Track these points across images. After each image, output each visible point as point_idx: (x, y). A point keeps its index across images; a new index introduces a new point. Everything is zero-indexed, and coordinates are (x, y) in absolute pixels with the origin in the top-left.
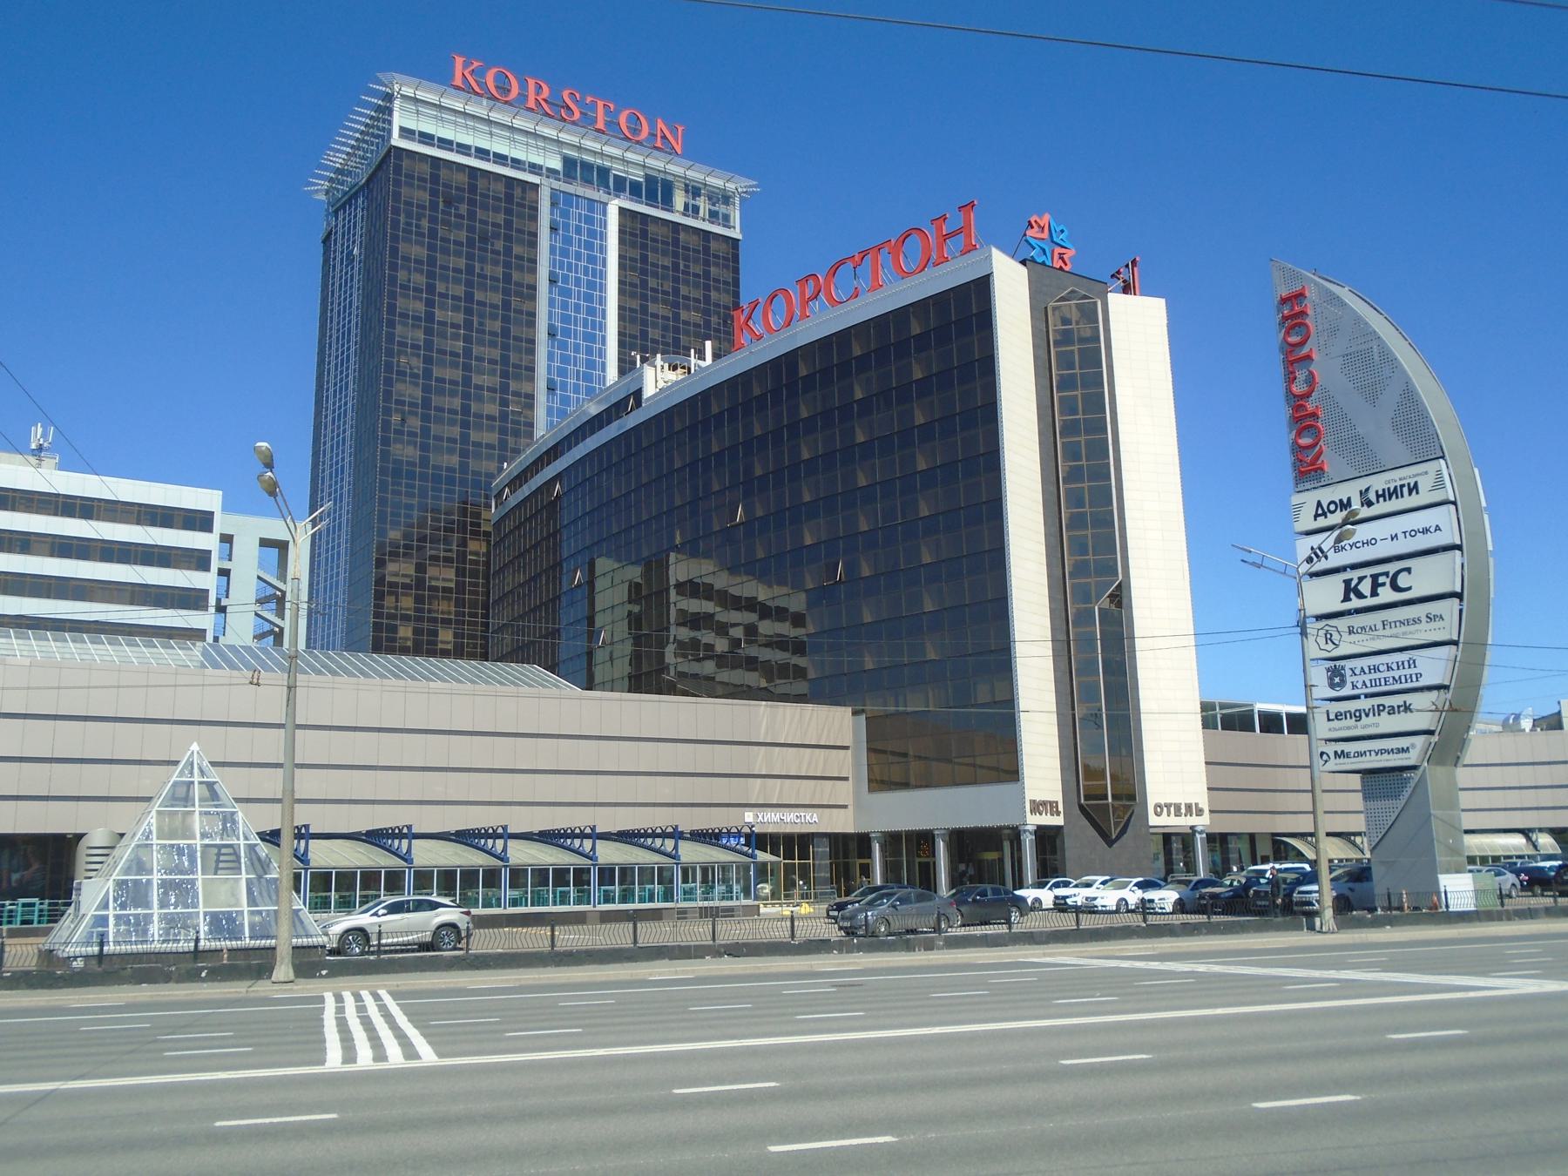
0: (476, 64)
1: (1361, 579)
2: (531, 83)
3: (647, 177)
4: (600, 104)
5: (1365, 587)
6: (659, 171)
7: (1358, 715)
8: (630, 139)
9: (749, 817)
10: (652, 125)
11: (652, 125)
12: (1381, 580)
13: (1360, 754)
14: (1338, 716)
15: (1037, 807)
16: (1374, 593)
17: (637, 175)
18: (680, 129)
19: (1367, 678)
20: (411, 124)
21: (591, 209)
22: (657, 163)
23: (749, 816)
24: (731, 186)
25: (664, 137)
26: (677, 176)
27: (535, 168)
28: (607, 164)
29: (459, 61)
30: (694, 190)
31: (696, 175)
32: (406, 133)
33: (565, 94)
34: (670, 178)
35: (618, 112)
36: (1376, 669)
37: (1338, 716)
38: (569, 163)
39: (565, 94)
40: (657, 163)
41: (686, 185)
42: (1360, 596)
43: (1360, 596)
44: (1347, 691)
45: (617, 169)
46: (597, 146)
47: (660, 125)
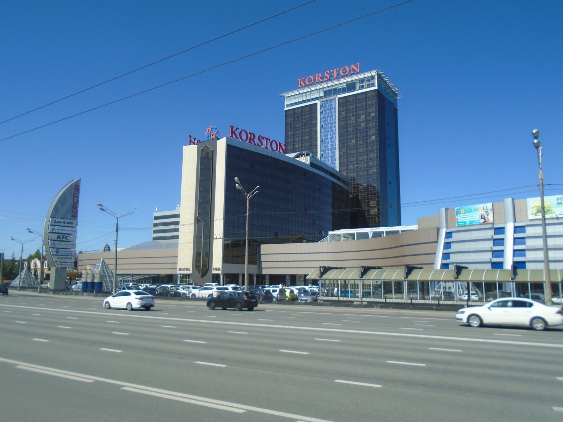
0: (303, 79)
1: (61, 236)
2: (317, 75)
3: (347, 85)
4: (335, 70)
5: (61, 237)
6: (351, 81)
8: (339, 77)
10: (350, 68)
11: (350, 68)
12: (64, 237)
13: (65, 265)
14: (59, 258)
15: (180, 269)
16: (63, 239)
17: (345, 86)
19: (63, 252)
20: (288, 103)
21: (331, 102)
22: (349, 79)
25: (354, 70)
27: (317, 99)
28: (336, 87)
29: (299, 80)
30: (362, 81)
31: (361, 76)
32: (287, 106)
33: (326, 74)
34: (354, 81)
35: (340, 70)
36: (65, 251)
37: (59, 258)
38: (325, 92)
39: (326, 74)
40: (349, 79)
41: (360, 81)
42: (60, 238)
43: (60, 238)
44: (59, 254)
45: (339, 87)
46: (332, 84)
47: (353, 66)
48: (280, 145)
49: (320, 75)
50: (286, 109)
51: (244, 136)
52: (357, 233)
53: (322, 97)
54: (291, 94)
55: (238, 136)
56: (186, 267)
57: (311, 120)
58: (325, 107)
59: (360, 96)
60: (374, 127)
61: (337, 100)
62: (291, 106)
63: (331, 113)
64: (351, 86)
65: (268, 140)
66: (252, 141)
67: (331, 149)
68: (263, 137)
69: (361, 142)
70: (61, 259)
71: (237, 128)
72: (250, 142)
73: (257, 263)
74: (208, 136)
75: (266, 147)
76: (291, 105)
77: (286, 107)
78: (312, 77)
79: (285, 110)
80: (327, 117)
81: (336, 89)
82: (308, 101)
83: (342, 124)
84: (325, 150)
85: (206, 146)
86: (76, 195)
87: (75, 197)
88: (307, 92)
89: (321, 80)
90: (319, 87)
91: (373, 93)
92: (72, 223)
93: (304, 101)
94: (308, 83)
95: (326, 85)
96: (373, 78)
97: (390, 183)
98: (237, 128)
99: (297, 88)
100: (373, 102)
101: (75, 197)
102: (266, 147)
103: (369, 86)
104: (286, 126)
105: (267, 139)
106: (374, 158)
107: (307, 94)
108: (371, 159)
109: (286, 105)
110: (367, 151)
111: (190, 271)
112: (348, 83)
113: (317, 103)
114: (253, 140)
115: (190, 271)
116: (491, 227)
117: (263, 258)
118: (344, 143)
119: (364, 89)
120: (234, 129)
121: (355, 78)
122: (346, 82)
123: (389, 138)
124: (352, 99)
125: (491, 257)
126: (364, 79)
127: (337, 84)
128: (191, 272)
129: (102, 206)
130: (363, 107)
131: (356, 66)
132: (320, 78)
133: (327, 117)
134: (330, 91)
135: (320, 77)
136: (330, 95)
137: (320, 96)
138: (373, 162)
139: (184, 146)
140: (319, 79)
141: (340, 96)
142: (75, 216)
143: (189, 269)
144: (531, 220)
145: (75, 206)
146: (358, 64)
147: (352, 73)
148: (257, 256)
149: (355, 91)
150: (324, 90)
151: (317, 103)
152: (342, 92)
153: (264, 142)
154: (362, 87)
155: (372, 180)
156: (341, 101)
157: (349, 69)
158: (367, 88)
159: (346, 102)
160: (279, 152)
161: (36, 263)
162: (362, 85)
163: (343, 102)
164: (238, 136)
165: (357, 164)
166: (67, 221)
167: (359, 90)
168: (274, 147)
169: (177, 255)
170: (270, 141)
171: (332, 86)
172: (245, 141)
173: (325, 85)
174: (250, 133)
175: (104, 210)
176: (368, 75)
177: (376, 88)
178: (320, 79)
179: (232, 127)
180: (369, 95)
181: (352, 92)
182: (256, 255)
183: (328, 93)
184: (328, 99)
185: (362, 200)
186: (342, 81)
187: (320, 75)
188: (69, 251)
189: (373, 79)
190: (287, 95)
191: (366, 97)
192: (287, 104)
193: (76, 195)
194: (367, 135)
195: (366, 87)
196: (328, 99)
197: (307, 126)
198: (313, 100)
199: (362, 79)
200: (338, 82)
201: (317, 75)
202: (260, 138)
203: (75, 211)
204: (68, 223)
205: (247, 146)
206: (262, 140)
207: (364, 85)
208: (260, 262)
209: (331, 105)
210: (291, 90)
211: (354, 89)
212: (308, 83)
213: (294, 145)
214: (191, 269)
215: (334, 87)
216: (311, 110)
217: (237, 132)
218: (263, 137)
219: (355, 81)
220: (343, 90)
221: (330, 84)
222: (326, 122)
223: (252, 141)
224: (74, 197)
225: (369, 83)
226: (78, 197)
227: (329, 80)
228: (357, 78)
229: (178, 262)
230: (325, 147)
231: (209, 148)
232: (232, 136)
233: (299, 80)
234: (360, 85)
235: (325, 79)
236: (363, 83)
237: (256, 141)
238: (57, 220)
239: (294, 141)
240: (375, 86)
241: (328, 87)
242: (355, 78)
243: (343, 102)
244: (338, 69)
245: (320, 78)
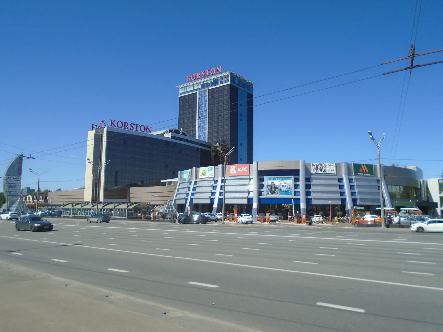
0: (190, 76)
3: (214, 81)
4: (207, 71)
7: (13, 197)
8: (210, 75)
17: (212, 81)
20: (181, 92)
22: (214, 77)
27: (197, 89)
30: (222, 78)
31: (221, 75)
33: (203, 74)
38: (202, 85)
39: (203, 74)
40: (214, 77)
45: (209, 82)
47: (217, 68)
48: (147, 128)
49: (199, 73)
50: (180, 96)
51: (120, 125)
52: (168, 182)
53: (200, 88)
54: (182, 86)
55: (116, 125)
57: (193, 104)
58: (201, 95)
59: (215, 90)
61: (208, 91)
62: (182, 94)
63: (205, 99)
64: (216, 82)
65: (138, 126)
66: (126, 127)
67: (204, 123)
68: (134, 124)
69: (221, 119)
70: (12, 197)
71: (115, 121)
72: (125, 128)
73: (128, 198)
74: (101, 125)
75: (137, 130)
76: (183, 93)
77: (180, 95)
78: (195, 75)
79: (179, 96)
80: (202, 102)
81: (207, 83)
82: (192, 91)
83: (210, 106)
84: (200, 124)
85: (98, 131)
86: (20, 163)
87: (20, 164)
88: (191, 85)
89: (200, 77)
90: (198, 82)
91: (228, 86)
92: (18, 178)
93: (190, 91)
94: (192, 79)
95: (202, 81)
96: (228, 76)
97: (241, 144)
98: (115, 121)
99: (185, 83)
100: (227, 92)
101: (20, 164)
102: (137, 130)
103: (226, 82)
104: (179, 107)
105: (137, 125)
106: (227, 129)
107: (192, 86)
108: (225, 130)
109: (180, 93)
112: (214, 79)
113: (196, 93)
114: (127, 126)
116: (188, 181)
117: (131, 195)
118: (211, 119)
120: (113, 121)
121: (218, 76)
122: (213, 79)
123: (241, 115)
124: (216, 90)
125: (211, 195)
126: (223, 77)
127: (208, 80)
129: (31, 170)
130: (222, 95)
131: (219, 68)
132: (199, 76)
133: (202, 102)
134: (204, 84)
135: (199, 75)
136: (204, 87)
137: (199, 88)
139: (88, 131)
140: (198, 76)
141: (210, 88)
142: (20, 174)
144: (201, 178)
145: (20, 169)
146: (220, 67)
147: (217, 72)
148: (128, 194)
149: (218, 85)
150: (201, 83)
151: (196, 93)
152: (214, 85)
153: (135, 127)
154: (222, 82)
156: (210, 91)
158: (225, 83)
159: (213, 92)
160: (147, 132)
161: (29, 198)
162: (222, 80)
163: (211, 92)
164: (116, 125)
165: (218, 133)
166: (15, 177)
167: (220, 84)
168: (143, 129)
169: (84, 193)
170: (139, 126)
171: (206, 81)
172: (121, 127)
173: (201, 81)
174: (125, 123)
175: (32, 172)
176: (225, 74)
177: (229, 83)
178: (199, 77)
179: (111, 120)
180: (226, 87)
182: (127, 194)
183: (203, 86)
184: (203, 90)
185: (220, 156)
186: (211, 78)
187: (199, 73)
188: (16, 193)
190: (180, 87)
191: (224, 89)
192: (180, 93)
193: (20, 163)
196: (203, 90)
197: (191, 107)
198: (194, 90)
200: (208, 79)
201: (197, 74)
202: (132, 125)
203: (20, 171)
204: (16, 178)
205: (122, 130)
206: (134, 126)
207: (223, 81)
208: (130, 198)
209: (205, 94)
210: (182, 84)
211: (217, 84)
212: (192, 79)
213: (183, 120)
215: (206, 82)
216: (193, 97)
217: (115, 123)
218: (134, 124)
219: (218, 78)
220: (212, 84)
221: (204, 80)
222: (201, 105)
223: (126, 127)
224: (19, 164)
225: (226, 80)
226: (22, 164)
227: (204, 77)
228: (219, 76)
229: (84, 198)
230: (201, 121)
231: (100, 133)
232: (111, 125)
233: (188, 77)
234: (221, 81)
235: (202, 77)
237: (129, 127)
238: (9, 177)
239: (183, 117)
240: (229, 82)
241: (203, 82)
242: (218, 76)
243: (211, 92)
244: (209, 70)
245: (199, 76)
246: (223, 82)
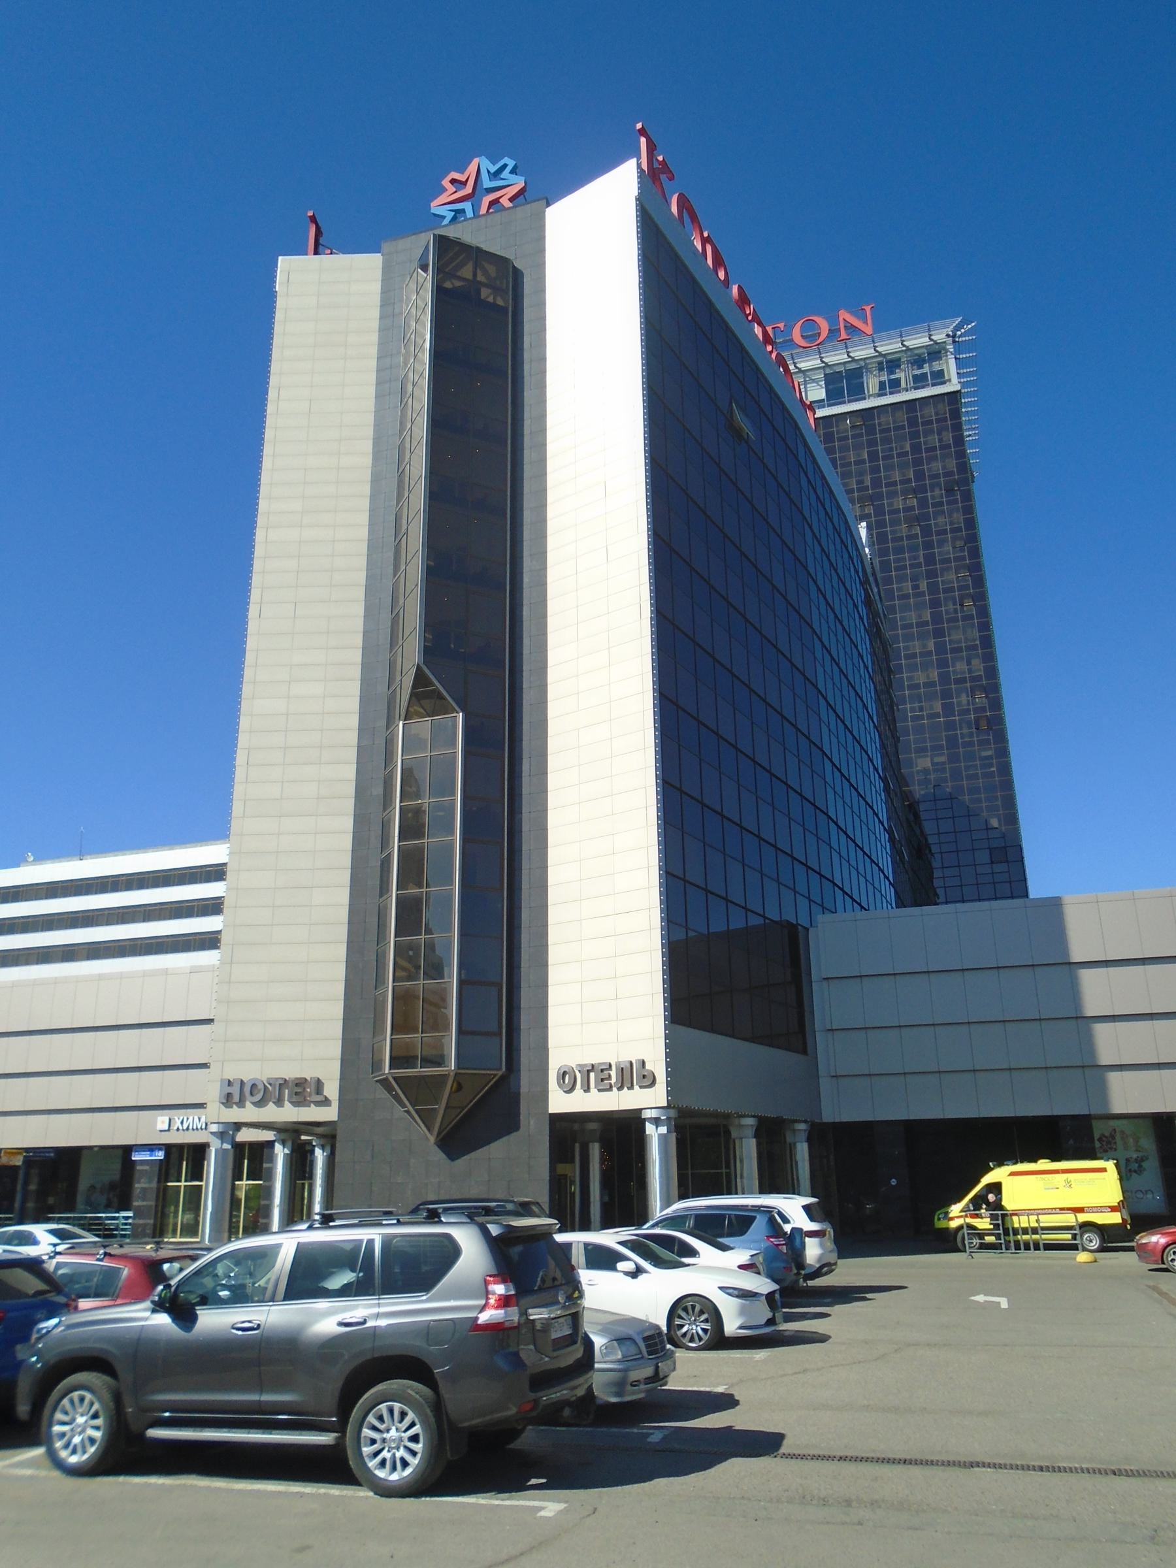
9: (162, 1121)
10: (833, 319)
11: (833, 319)
18: (868, 309)
23: (163, 1122)
24: (940, 336)
25: (851, 328)
26: (865, 359)
30: (891, 364)
31: (890, 346)
47: (844, 315)
56: (291, 1072)
60: (959, 529)
96: (935, 352)
103: (919, 381)
110: (937, 618)
111: (326, 1102)
115: (326, 1102)
119: (899, 392)
126: (899, 359)
128: (329, 1114)
138: (969, 663)
143: (319, 1084)
146: (868, 309)
154: (895, 385)
155: (971, 735)
157: (830, 326)
158: (916, 388)
167: (880, 395)
176: (918, 341)
181: (850, 401)
189: (940, 358)
191: (913, 422)
194: (930, 559)
195: (912, 385)
199: (890, 357)
211: (858, 392)
214: (332, 1090)
219: (862, 363)
234: (884, 378)
236: (892, 373)
240: (950, 380)
242: (862, 352)
246: (903, 384)
